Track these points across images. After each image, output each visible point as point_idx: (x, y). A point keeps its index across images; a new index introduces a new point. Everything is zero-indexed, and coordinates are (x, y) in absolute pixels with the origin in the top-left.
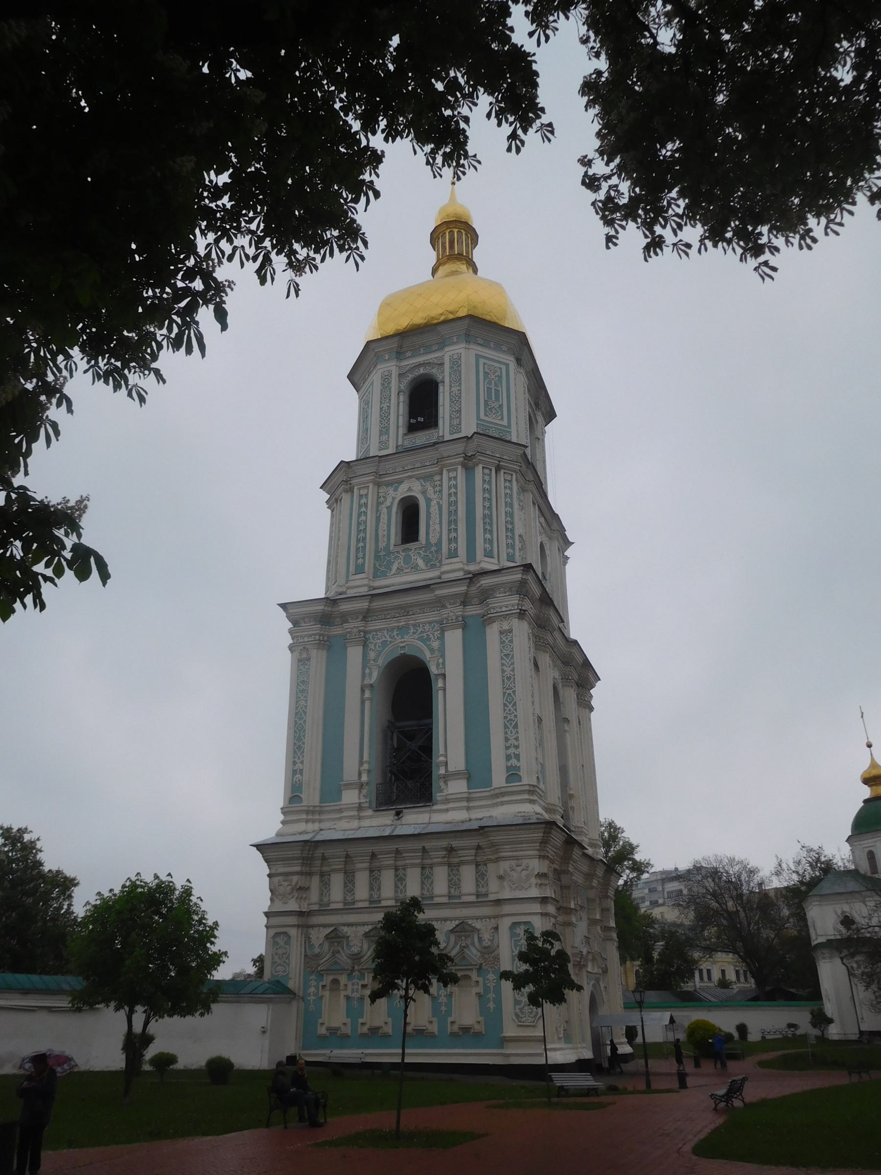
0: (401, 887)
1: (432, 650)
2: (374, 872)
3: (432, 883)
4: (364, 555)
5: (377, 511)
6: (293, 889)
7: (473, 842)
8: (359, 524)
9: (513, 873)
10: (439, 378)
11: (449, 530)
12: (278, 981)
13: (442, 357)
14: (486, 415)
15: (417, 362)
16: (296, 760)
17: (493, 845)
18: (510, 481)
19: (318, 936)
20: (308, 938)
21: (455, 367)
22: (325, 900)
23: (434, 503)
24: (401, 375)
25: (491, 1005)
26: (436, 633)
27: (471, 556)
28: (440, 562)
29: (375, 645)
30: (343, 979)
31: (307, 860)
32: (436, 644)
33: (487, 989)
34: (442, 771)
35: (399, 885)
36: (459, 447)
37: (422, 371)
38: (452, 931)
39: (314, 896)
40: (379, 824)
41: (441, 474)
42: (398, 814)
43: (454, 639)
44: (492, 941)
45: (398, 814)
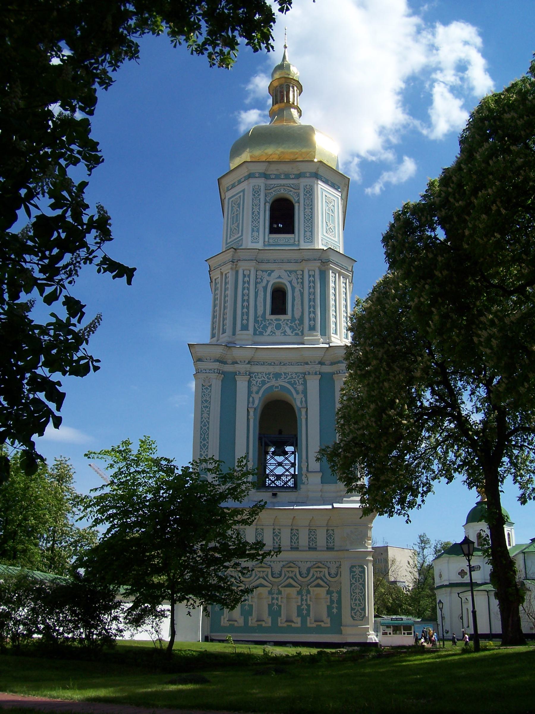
0: (277, 540)
1: (298, 393)
3: (298, 538)
4: (248, 318)
5: (256, 287)
8: (243, 295)
16: (202, 453)
21: (308, 195)
23: (297, 290)
25: (335, 611)
26: (300, 380)
27: (325, 331)
29: (257, 381)
32: (300, 388)
33: (332, 602)
35: (275, 538)
37: (282, 191)
41: (303, 271)
43: (313, 385)
44: (337, 575)
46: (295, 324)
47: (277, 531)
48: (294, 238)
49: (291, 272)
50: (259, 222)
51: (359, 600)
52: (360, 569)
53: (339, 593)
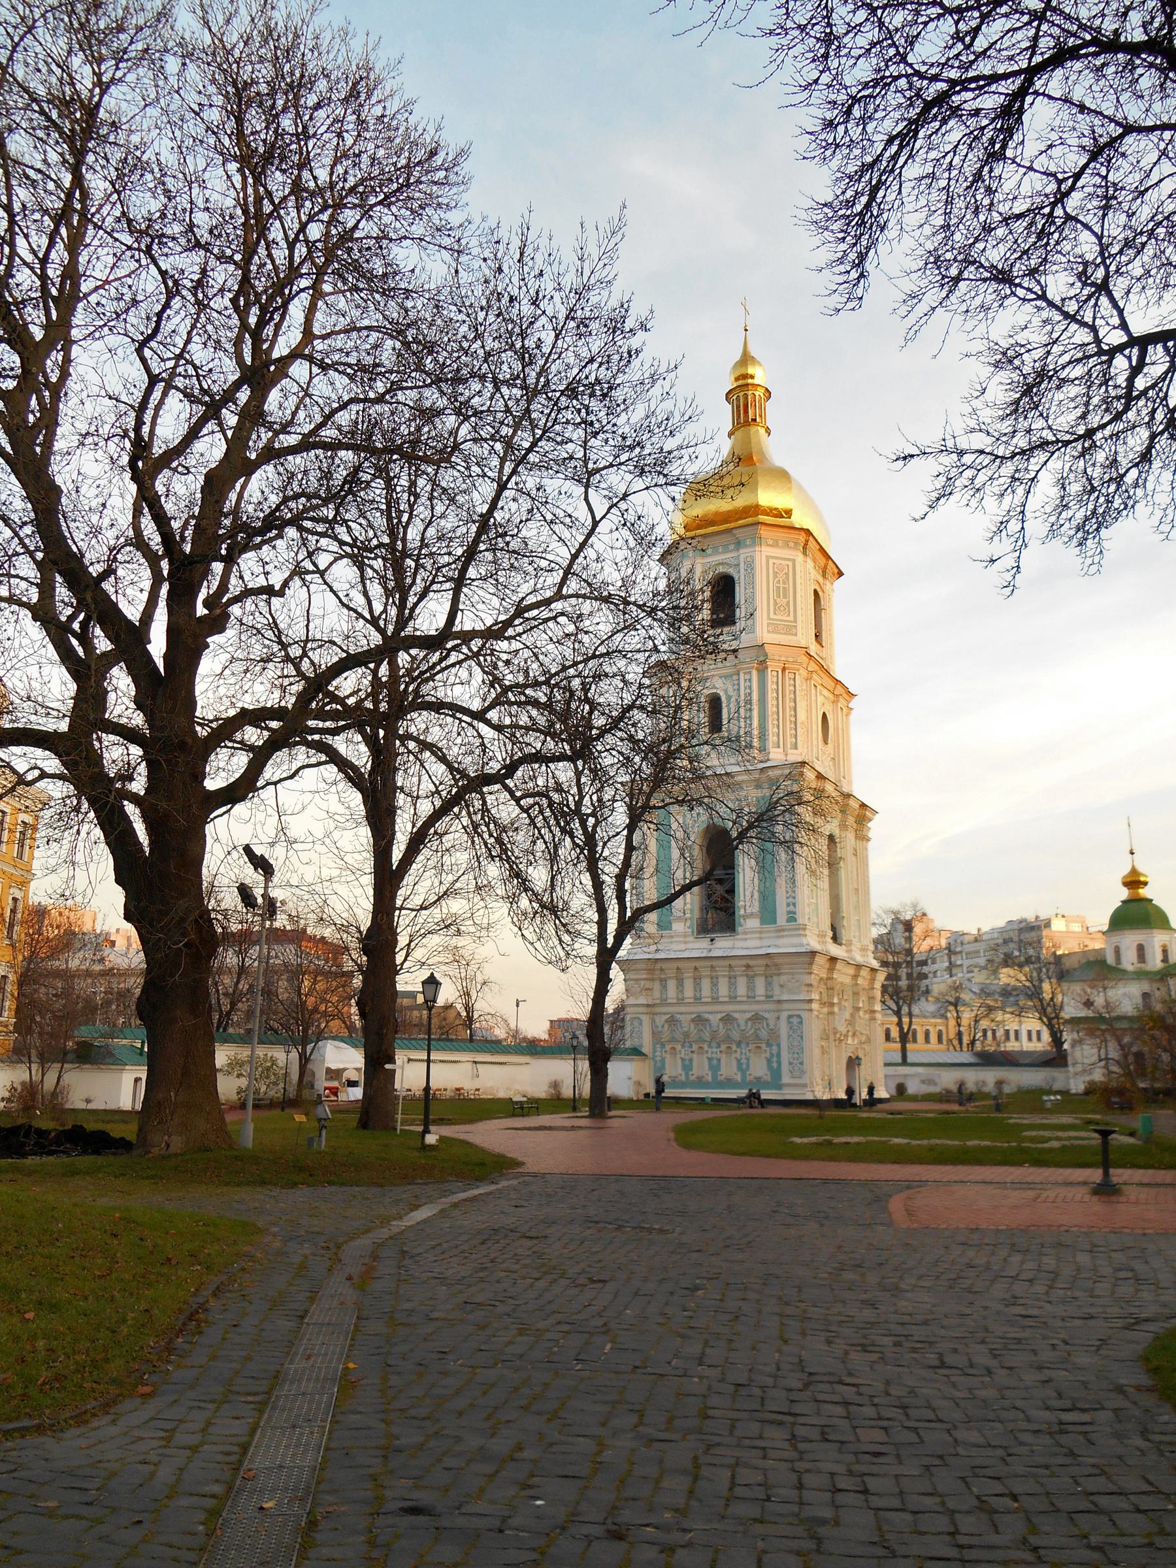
2: (697, 980)
7: (763, 962)
17: (776, 965)
19: (660, 1020)
20: (653, 1021)
30: (679, 1047)
31: (651, 971)
34: (742, 912)
37: (721, 569)
39: (657, 994)
40: (699, 947)
53: (779, 1045)
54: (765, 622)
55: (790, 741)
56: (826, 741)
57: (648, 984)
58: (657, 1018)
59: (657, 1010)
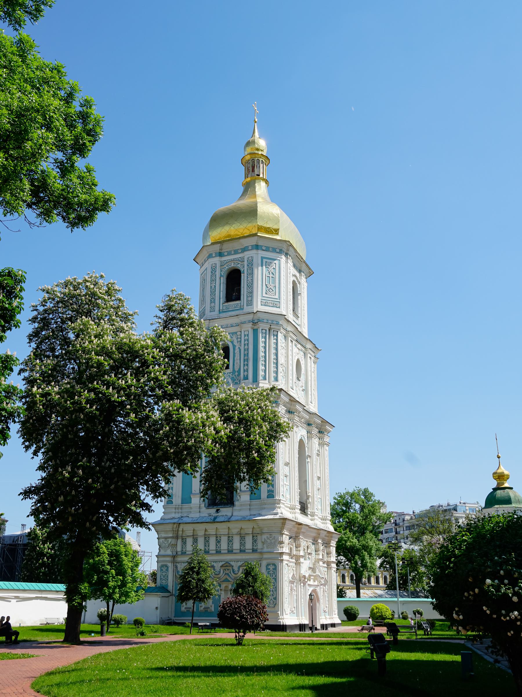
6: (169, 545)
9: (268, 541)
10: (242, 270)
11: (244, 365)
12: (163, 587)
13: (243, 258)
14: (266, 294)
15: (231, 261)
18: (277, 336)
20: (176, 567)
22: (184, 550)
23: (237, 348)
24: (221, 266)
27: (255, 380)
28: (240, 381)
36: (250, 317)
37: (233, 265)
38: (240, 566)
39: (179, 549)
41: (241, 332)
42: (217, 511)
45: (217, 511)
46: (235, 375)
47: (219, 538)
48: (241, 303)
49: (233, 334)
50: (215, 294)
51: (273, 591)
52: (273, 567)
54: (260, 298)
55: (273, 375)
56: (298, 379)
57: (173, 541)
58: (179, 565)
59: (179, 559)
